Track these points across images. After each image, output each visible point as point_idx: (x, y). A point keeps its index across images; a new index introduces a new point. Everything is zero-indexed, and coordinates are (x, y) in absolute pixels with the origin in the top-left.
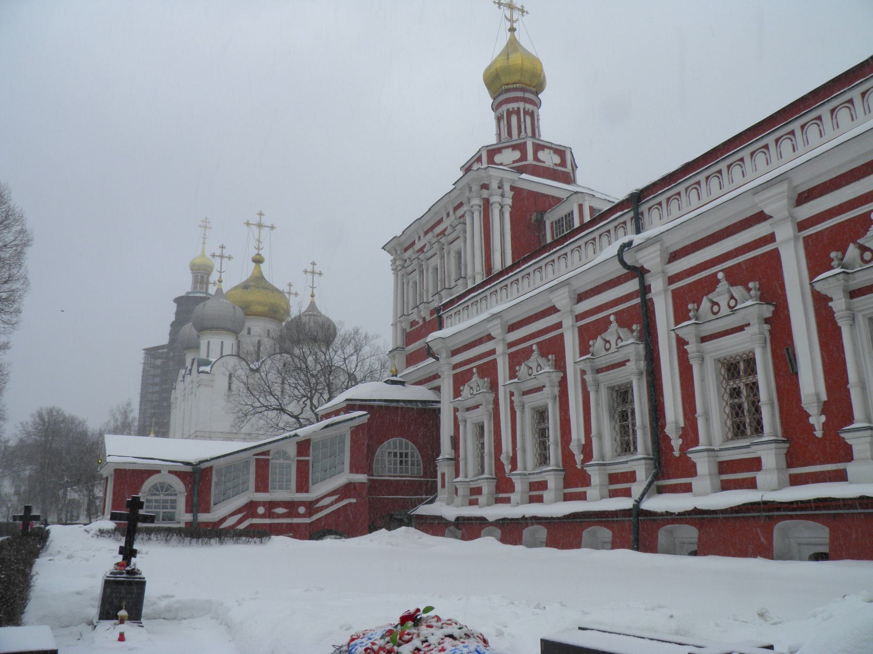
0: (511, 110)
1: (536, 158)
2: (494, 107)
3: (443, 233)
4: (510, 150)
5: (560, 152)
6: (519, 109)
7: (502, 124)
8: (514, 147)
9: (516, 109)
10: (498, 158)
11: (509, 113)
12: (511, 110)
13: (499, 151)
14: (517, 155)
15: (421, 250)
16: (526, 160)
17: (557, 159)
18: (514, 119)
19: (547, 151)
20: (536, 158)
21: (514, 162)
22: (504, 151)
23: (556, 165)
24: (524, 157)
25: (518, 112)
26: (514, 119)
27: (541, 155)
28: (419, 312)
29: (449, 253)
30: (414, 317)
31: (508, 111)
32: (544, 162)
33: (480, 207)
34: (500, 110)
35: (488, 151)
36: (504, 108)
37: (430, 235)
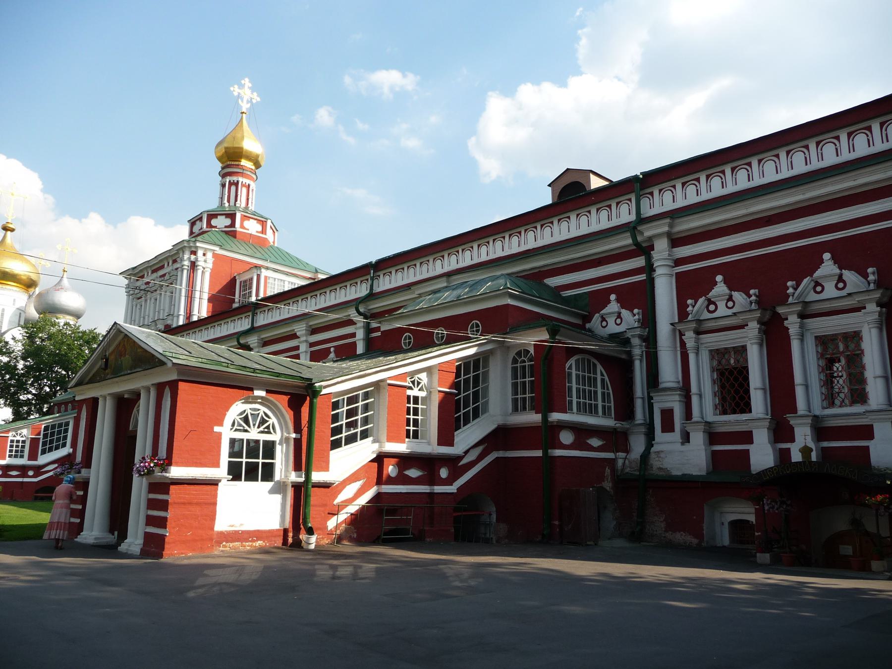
1: (242, 226)
4: (224, 217)
6: (238, 181)
8: (228, 216)
9: (236, 182)
10: (214, 222)
12: (232, 181)
14: (228, 222)
16: (234, 227)
17: (259, 228)
18: (233, 188)
20: (242, 226)
21: (226, 227)
23: (257, 232)
26: (233, 188)
27: (247, 224)
32: (248, 230)
33: (188, 267)
35: (208, 215)
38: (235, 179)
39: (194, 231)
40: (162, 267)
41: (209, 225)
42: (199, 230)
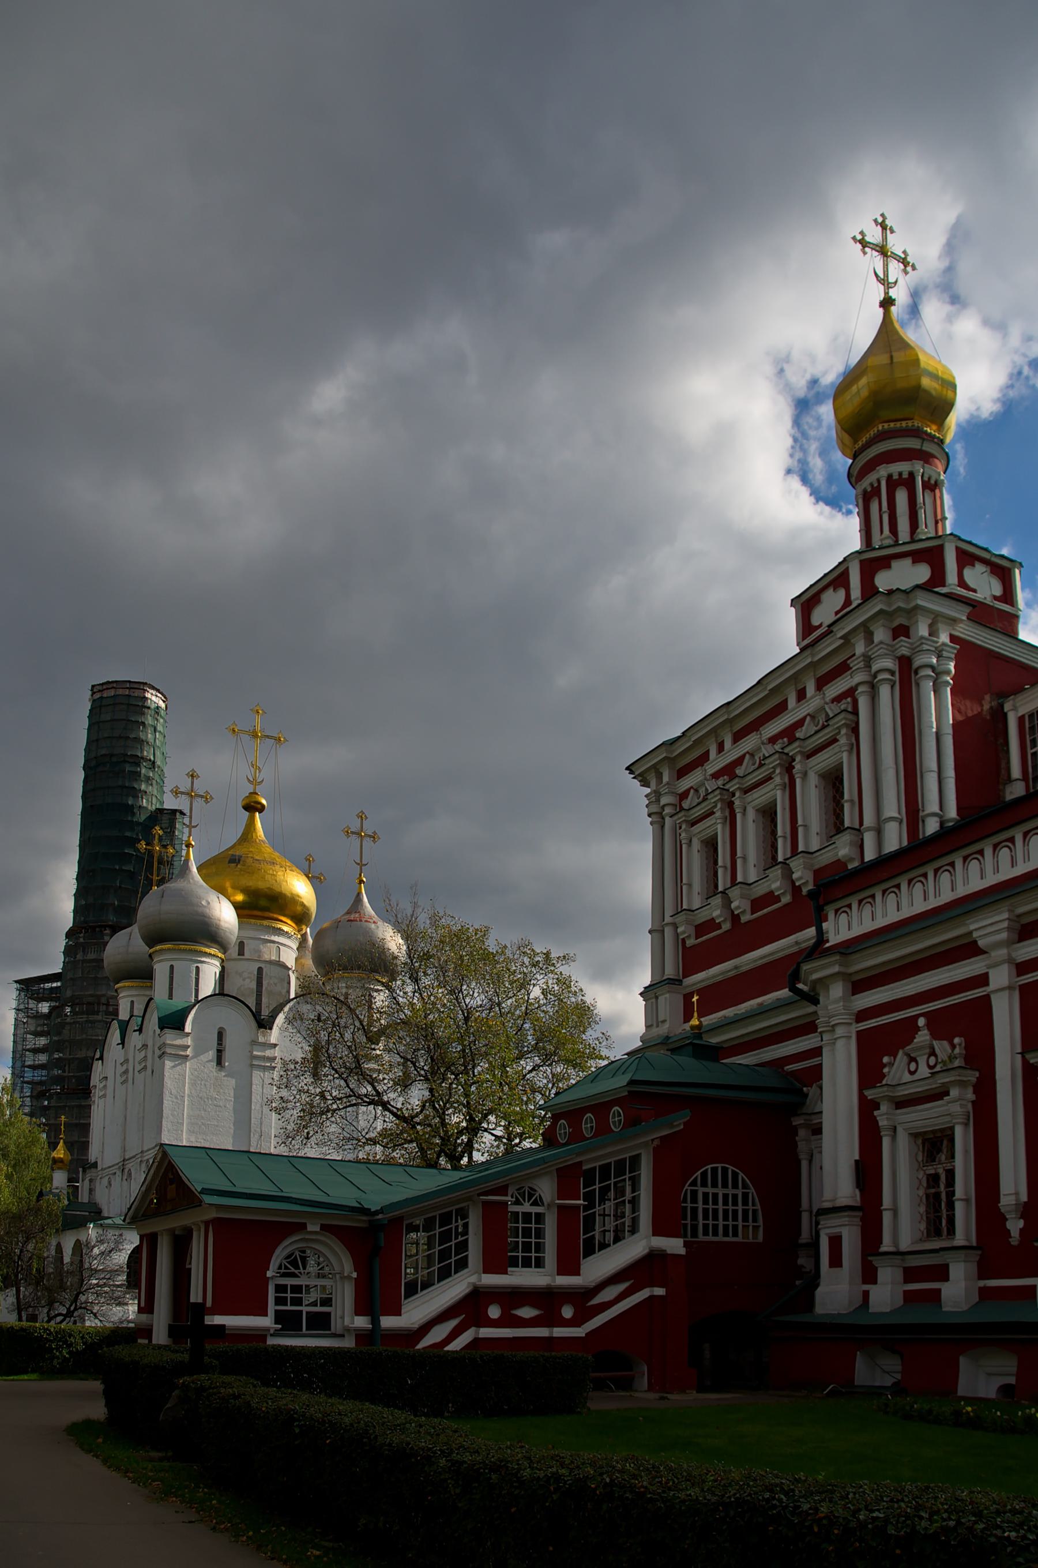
0: (896, 477)
2: (855, 473)
3: (789, 733)
4: (908, 561)
5: (1002, 571)
6: (912, 475)
7: (874, 507)
8: (917, 557)
9: (905, 476)
10: (883, 581)
11: (893, 484)
12: (896, 477)
13: (884, 563)
14: (922, 573)
15: (729, 771)
18: (901, 497)
19: (980, 568)
20: (962, 584)
22: (895, 564)
23: (995, 598)
24: (938, 577)
25: (909, 482)
26: (901, 497)
28: (727, 901)
29: (805, 774)
30: (715, 911)
31: (890, 477)
34: (871, 478)
35: (862, 562)
36: (882, 472)
37: (750, 743)
38: (902, 468)
39: (815, 621)
40: (781, 708)
41: (869, 591)
42: (837, 613)
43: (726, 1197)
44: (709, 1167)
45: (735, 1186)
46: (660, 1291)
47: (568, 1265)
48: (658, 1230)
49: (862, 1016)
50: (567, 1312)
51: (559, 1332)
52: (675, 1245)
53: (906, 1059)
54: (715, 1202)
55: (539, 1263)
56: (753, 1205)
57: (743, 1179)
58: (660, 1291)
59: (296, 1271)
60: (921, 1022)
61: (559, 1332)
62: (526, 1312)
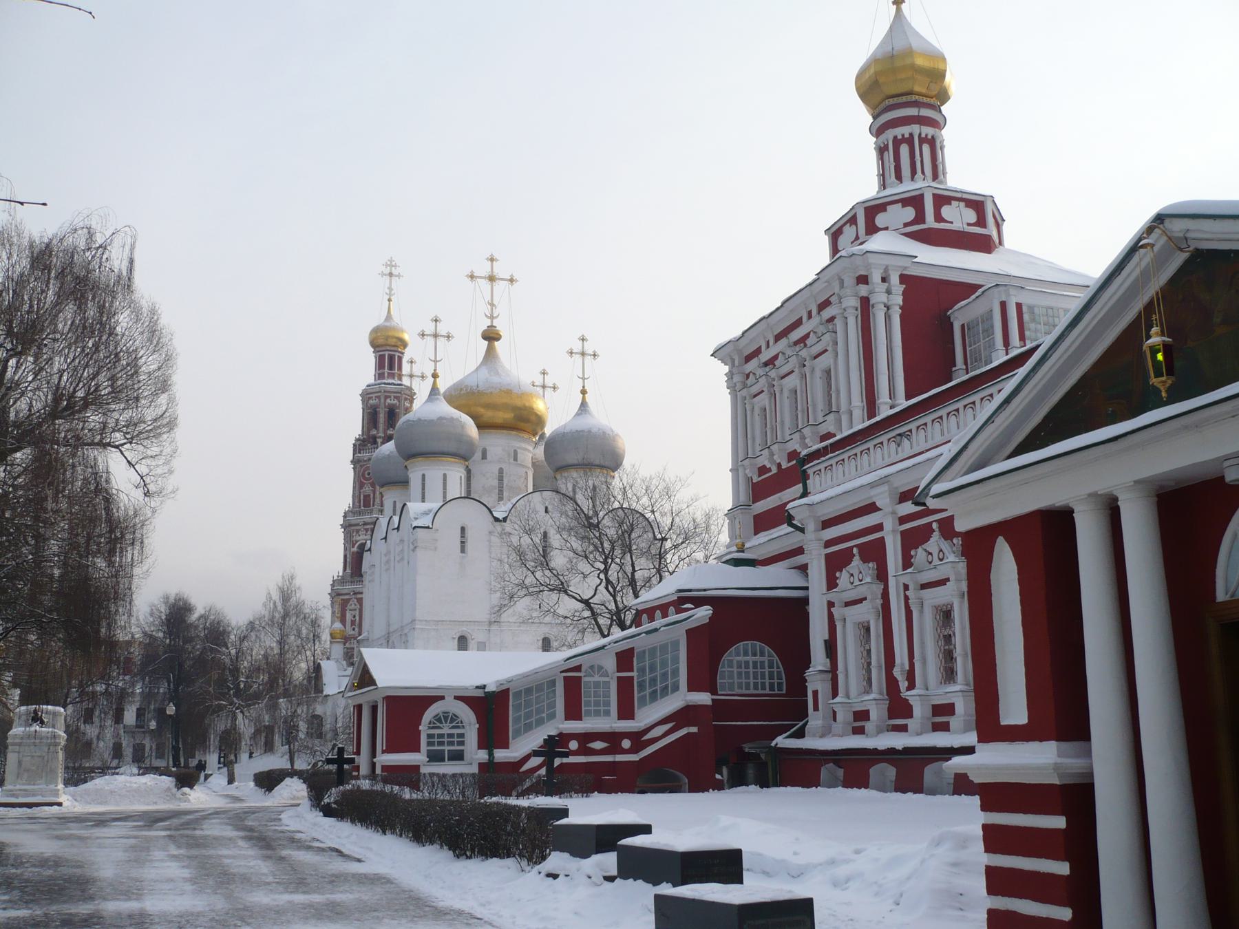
43: (755, 663)
44: (742, 643)
45: (762, 654)
46: (694, 729)
47: (626, 712)
48: (692, 687)
49: (828, 544)
50: (626, 744)
51: (620, 758)
52: (704, 698)
53: (848, 575)
54: (762, 667)
55: (607, 713)
56: (778, 667)
57: (769, 652)
58: (694, 729)
59: (441, 725)
60: (855, 551)
61: (620, 758)
62: (598, 745)
